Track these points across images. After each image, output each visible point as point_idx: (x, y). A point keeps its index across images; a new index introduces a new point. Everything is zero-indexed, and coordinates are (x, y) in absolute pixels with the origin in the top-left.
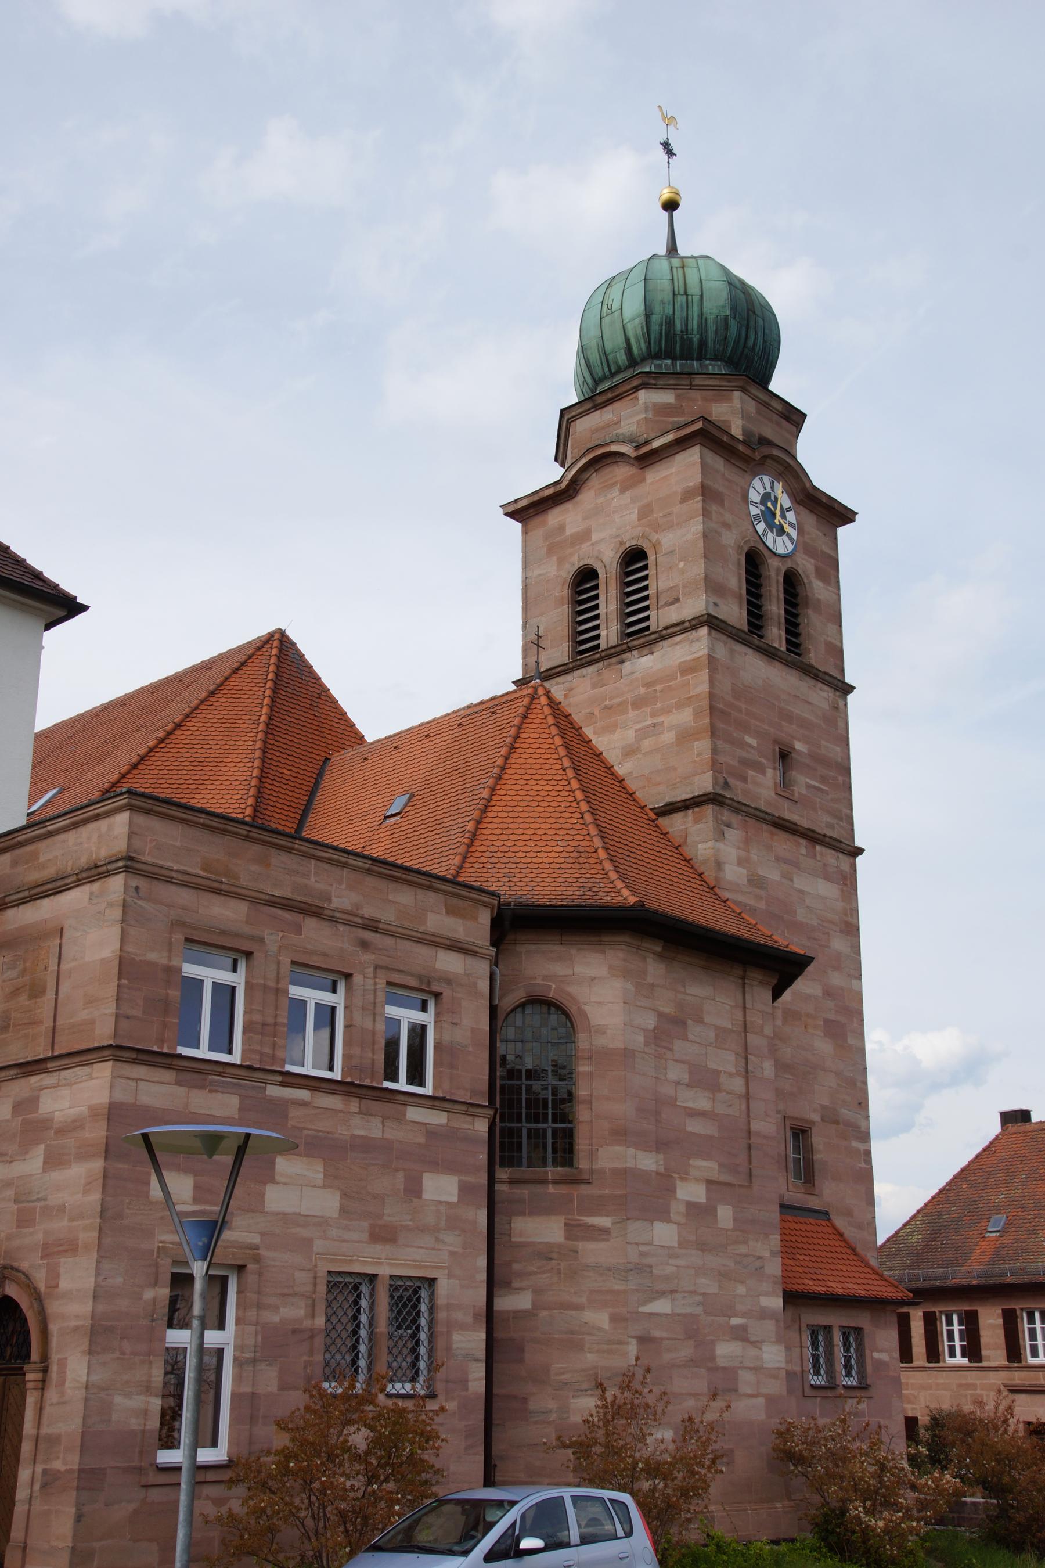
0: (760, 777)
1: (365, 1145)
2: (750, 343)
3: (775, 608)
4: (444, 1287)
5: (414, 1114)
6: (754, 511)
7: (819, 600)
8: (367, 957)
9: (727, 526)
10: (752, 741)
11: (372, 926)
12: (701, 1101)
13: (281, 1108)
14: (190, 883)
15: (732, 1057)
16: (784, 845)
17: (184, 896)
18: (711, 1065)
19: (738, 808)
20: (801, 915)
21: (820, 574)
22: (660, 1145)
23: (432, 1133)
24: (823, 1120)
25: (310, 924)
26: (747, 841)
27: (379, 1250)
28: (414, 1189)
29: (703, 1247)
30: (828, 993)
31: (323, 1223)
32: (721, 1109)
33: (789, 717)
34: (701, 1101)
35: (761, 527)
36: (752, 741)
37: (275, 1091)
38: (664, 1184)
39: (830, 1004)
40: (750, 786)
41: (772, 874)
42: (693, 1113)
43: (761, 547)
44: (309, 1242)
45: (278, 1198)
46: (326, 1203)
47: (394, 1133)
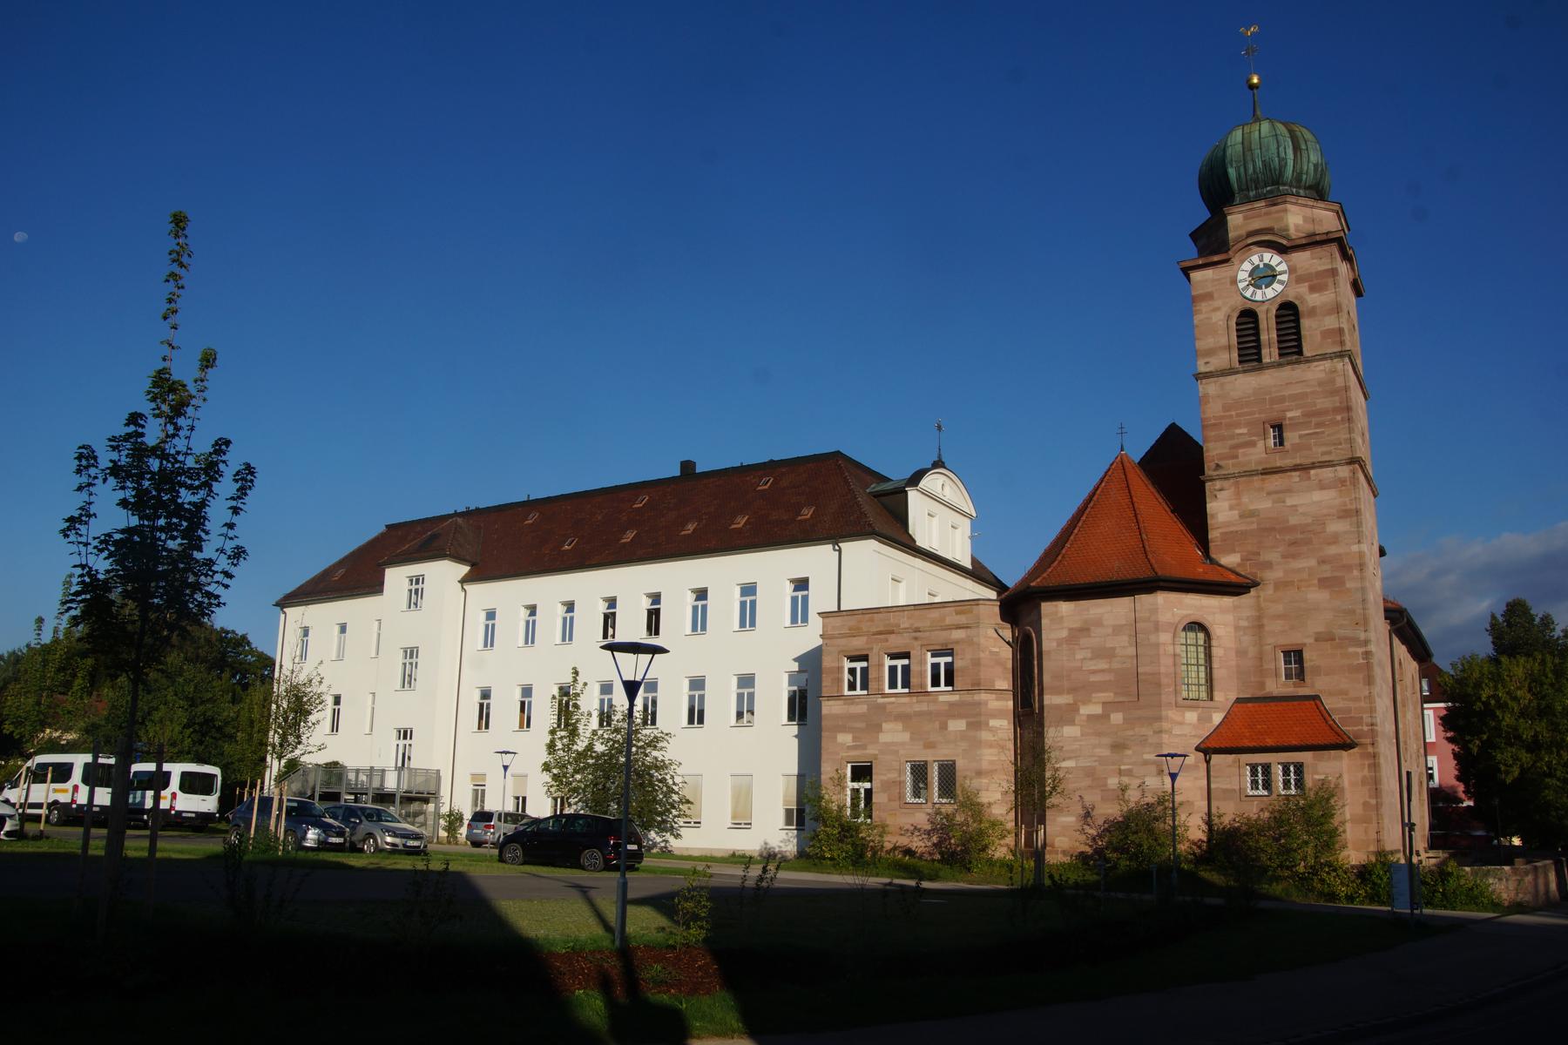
0: (1251, 450)
1: (920, 714)
2: (1251, 170)
3: (1269, 333)
4: (960, 764)
5: (942, 698)
6: (1241, 285)
7: (1314, 308)
8: (917, 644)
9: (1218, 309)
10: (1244, 431)
11: (917, 630)
12: (1103, 665)
13: (883, 706)
14: (843, 636)
15: (1126, 638)
16: (1275, 482)
17: (843, 642)
18: (1109, 645)
19: (1226, 478)
20: (1293, 521)
21: (1313, 289)
22: (1073, 690)
23: (951, 704)
24: (1316, 640)
25: (892, 637)
26: (1238, 494)
27: (929, 751)
28: (944, 727)
29: (1099, 734)
30: (1322, 561)
31: (903, 744)
32: (1116, 665)
33: (1282, 399)
34: (1103, 665)
35: (1248, 294)
36: (1244, 431)
37: (881, 700)
38: (1073, 708)
39: (1326, 567)
40: (1241, 459)
41: (1264, 505)
42: (1094, 672)
43: (1249, 305)
44: (897, 752)
45: (884, 738)
46: (906, 737)
47: (933, 707)
